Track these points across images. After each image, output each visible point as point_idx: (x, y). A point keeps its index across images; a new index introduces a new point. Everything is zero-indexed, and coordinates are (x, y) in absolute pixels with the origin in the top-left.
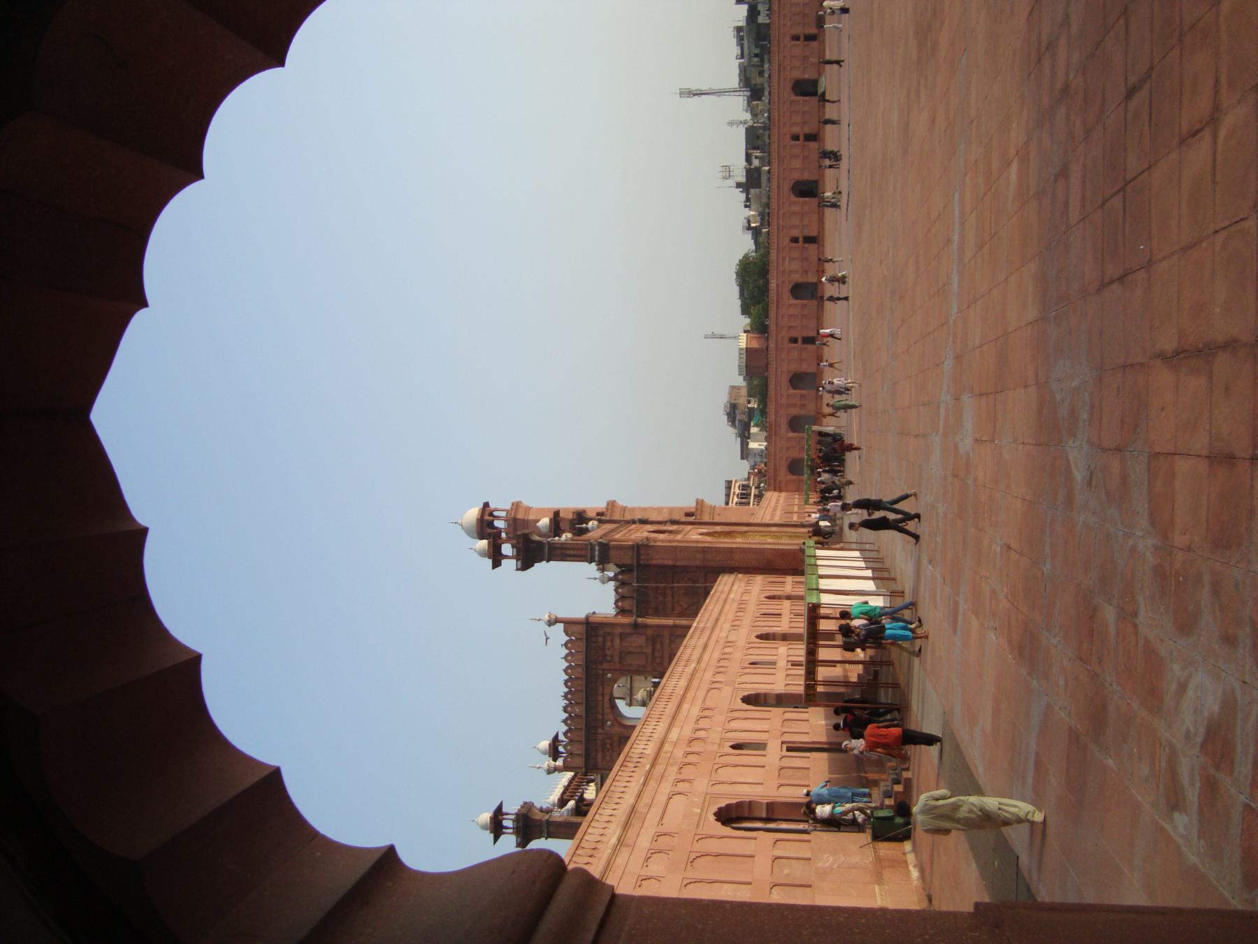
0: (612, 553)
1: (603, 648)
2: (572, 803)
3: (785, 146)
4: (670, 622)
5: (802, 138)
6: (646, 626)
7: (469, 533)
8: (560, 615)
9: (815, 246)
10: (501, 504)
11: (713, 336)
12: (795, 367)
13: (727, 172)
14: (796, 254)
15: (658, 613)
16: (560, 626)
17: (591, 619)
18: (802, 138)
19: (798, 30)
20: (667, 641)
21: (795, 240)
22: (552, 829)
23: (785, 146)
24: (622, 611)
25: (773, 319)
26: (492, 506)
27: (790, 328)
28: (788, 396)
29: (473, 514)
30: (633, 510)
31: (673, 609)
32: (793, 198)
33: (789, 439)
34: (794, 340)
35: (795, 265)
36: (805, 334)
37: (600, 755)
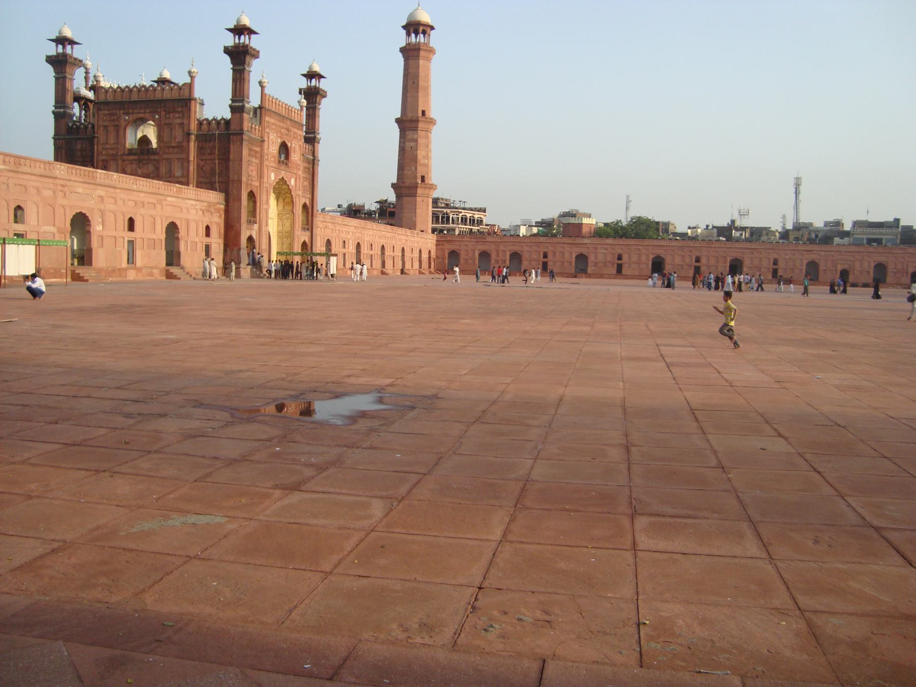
0: (238, 115)
1: (174, 112)
2: (90, 95)
4: (191, 158)
5: (697, 264)
6: (188, 142)
7: (411, 15)
8: (196, 81)
9: (615, 272)
10: (434, 39)
12: (526, 256)
13: (743, 214)
14: (609, 258)
15: (200, 150)
16: (188, 80)
17: (193, 102)
18: (697, 264)
19: (781, 264)
20: (179, 156)
21: (620, 257)
22: (61, 80)
24: (200, 123)
26: (432, 32)
27: (555, 253)
29: (424, 17)
30: (427, 137)
31: (202, 160)
32: (651, 257)
33: (474, 251)
34: (545, 256)
35: (601, 257)
36: (550, 264)
37: (106, 112)
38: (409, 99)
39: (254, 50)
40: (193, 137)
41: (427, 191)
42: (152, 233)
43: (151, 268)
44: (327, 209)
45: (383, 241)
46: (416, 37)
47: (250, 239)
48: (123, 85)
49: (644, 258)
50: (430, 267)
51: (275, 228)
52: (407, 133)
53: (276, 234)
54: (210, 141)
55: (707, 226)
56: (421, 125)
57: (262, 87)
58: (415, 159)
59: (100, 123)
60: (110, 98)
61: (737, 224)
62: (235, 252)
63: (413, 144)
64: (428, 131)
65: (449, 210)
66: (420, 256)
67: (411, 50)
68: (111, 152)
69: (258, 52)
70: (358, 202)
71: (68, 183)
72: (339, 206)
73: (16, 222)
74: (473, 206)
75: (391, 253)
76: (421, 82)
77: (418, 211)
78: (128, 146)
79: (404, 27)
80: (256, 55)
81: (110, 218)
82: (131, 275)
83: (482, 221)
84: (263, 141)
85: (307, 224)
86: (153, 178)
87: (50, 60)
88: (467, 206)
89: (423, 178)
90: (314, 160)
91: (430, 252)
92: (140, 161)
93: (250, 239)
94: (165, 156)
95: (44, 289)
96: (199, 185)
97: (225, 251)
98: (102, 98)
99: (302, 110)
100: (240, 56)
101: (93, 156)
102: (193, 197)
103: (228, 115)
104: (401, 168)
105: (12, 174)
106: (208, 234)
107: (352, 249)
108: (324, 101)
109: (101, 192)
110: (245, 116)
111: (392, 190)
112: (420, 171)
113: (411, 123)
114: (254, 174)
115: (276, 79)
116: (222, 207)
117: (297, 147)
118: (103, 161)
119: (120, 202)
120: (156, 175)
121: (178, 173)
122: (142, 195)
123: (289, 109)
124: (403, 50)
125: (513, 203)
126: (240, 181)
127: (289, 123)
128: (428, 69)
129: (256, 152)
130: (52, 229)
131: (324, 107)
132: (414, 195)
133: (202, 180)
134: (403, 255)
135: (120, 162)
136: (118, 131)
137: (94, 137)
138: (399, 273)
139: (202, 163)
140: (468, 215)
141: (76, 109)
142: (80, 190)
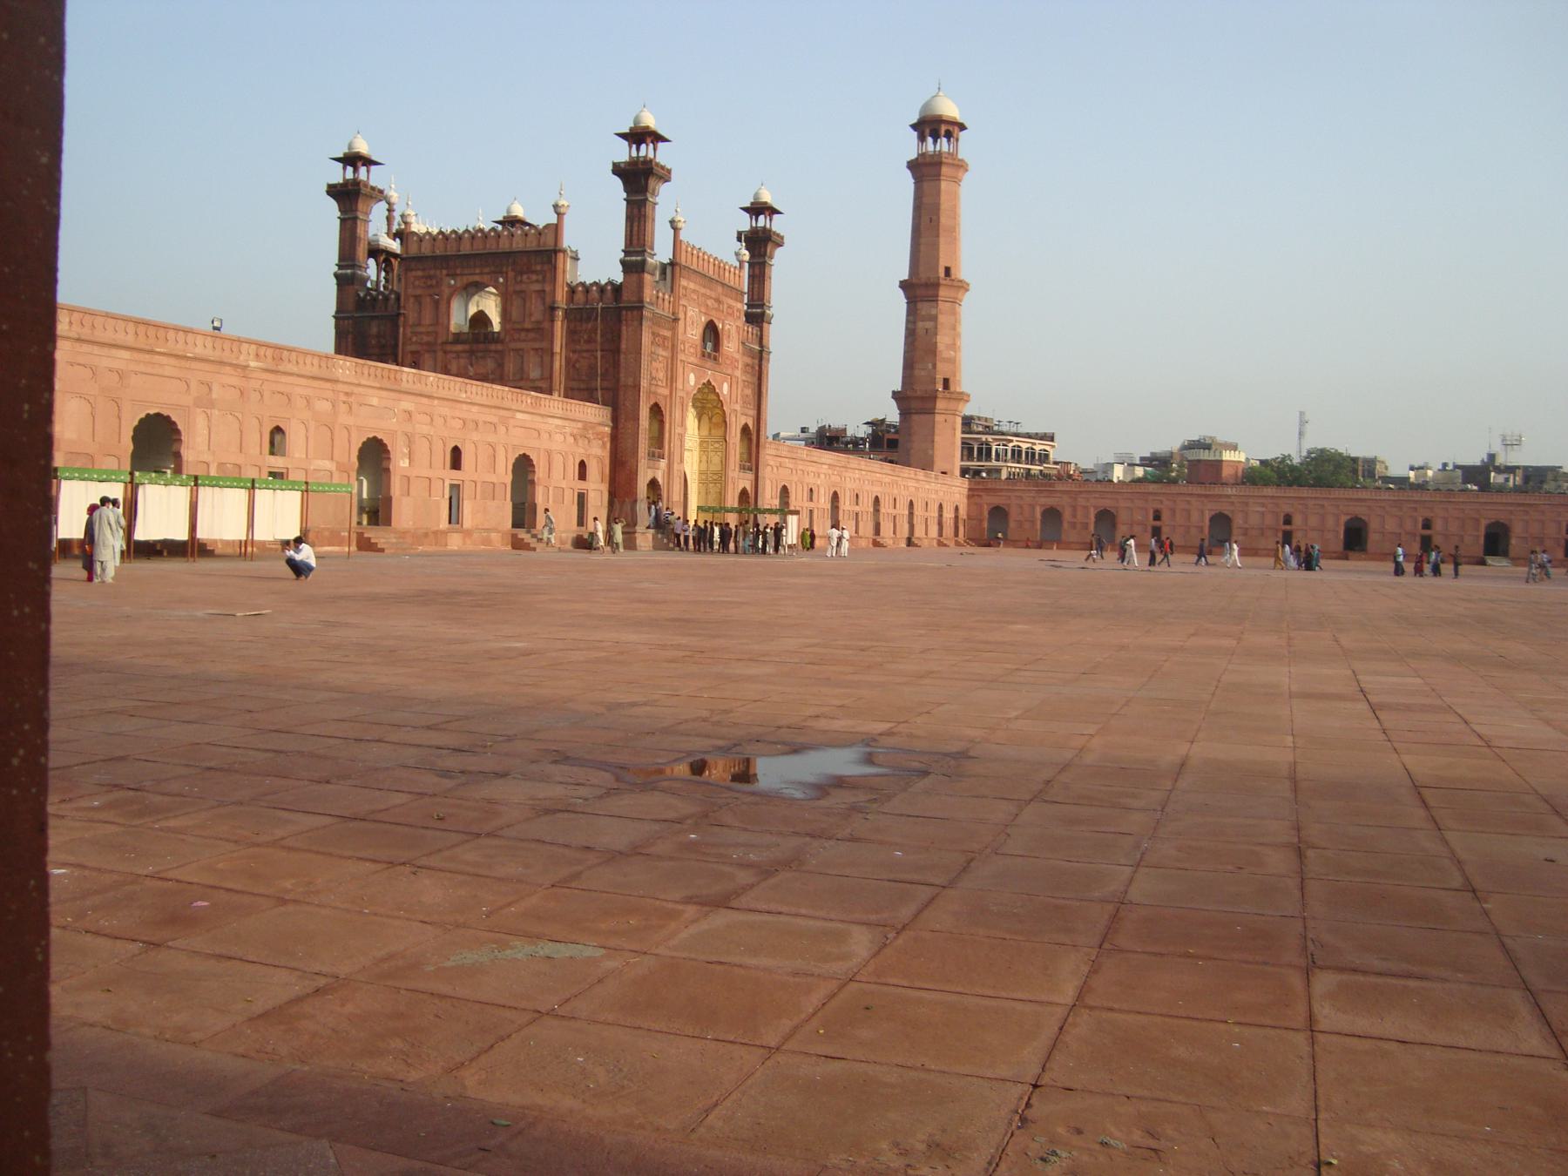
0: (634, 277)
2: (395, 246)
3: (1415, 509)
4: (557, 349)
5: (1427, 532)
7: (926, 106)
8: (566, 220)
10: (966, 146)
11: (1303, 422)
12: (1123, 516)
14: (1269, 520)
15: (572, 334)
16: (553, 219)
18: (1427, 532)
20: (537, 345)
21: (1288, 520)
22: (349, 223)
23: (1415, 509)
24: (572, 290)
25: (1184, 490)
26: (962, 135)
27: (1173, 511)
28: (1086, 508)
29: (949, 109)
30: (954, 313)
32: (1344, 519)
33: (1032, 507)
34: (1157, 517)
35: (1254, 520)
37: (420, 273)
38: (922, 248)
39: (663, 168)
40: (560, 313)
41: (952, 405)
42: (489, 474)
43: (487, 530)
44: (783, 434)
45: (877, 490)
46: (935, 142)
47: (653, 484)
48: (448, 229)
49: (1330, 522)
50: (956, 534)
51: (696, 467)
52: (920, 305)
53: (696, 477)
54: (589, 319)
55: (1445, 465)
56: (943, 292)
57: (676, 229)
58: (932, 351)
59: (410, 291)
60: (426, 250)
61: (1500, 461)
62: (627, 507)
63: (929, 325)
64: (955, 302)
65: (990, 438)
66: (941, 516)
67: (926, 164)
68: (426, 339)
69: (669, 171)
70: (836, 423)
71: (357, 390)
72: (804, 430)
73: (272, 453)
74: (1032, 431)
75: (891, 511)
76: (943, 220)
77: (937, 438)
78: (453, 329)
79: (914, 127)
80: (665, 176)
81: (422, 447)
82: (455, 542)
83: (1047, 456)
84: (676, 320)
85: (749, 460)
86: (493, 382)
87: (333, 191)
88: (1022, 430)
89: (946, 382)
90: (761, 352)
91: (957, 509)
92: (472, 352)
93: (653, 484)
94: (513, 345)
95: (313, 562)
96: (570, 393)
97: (611, 504)
98: (413, 250)
99: (741, 267)
100: (639, 179)
101: (397, 345)
102: (560, 413)
103: (619, 277)
104: (909, 365)
105: (265, 376)
106: (582, 475)
107: (824, 502)
108: (779, 252)
109: (407, 404)
110: (647, 277)
111: (893, 403)
112: (942, 371)
113: (927, 288)
114: (661, 375)
115: (699, 216)
116: (607, 430)
117: (734, 330)
118: (413, 353)
119: (439, 421)
120: (497, 377)
121: (534, 373)
122: (475, 409)
123: (720, 266)
124: (913, 166)
125: (1102, 427)
126: (637, 387)
127: (720, 289)
128: (955, 197)
129: (665, 338)
130: (328, 465)
131: (780, 263)
132: (931, 412)
133: (574, 384)
134: (911, 514)
135: (440, 354)
136: (437, 303)
137: (399, 315)
138: (903, 545)
139: (574, 357)
140: (1024, 446)
141: (372, 269)
142: (375, 401)
